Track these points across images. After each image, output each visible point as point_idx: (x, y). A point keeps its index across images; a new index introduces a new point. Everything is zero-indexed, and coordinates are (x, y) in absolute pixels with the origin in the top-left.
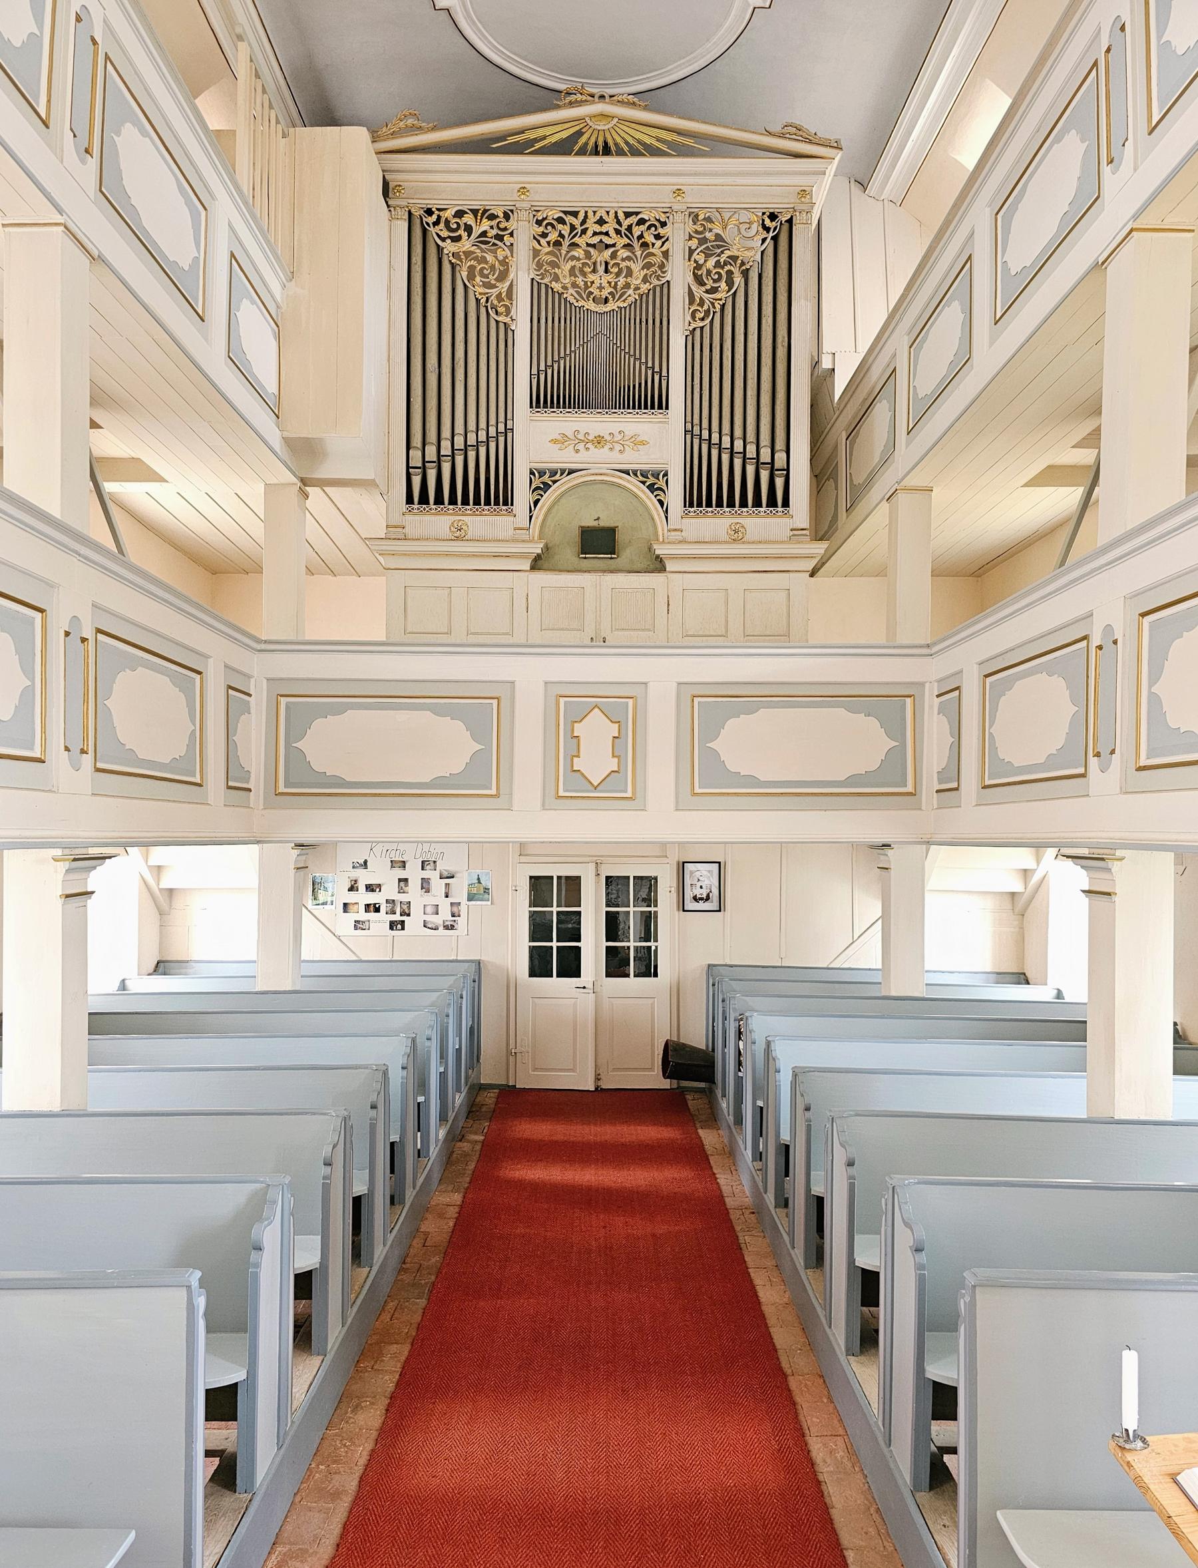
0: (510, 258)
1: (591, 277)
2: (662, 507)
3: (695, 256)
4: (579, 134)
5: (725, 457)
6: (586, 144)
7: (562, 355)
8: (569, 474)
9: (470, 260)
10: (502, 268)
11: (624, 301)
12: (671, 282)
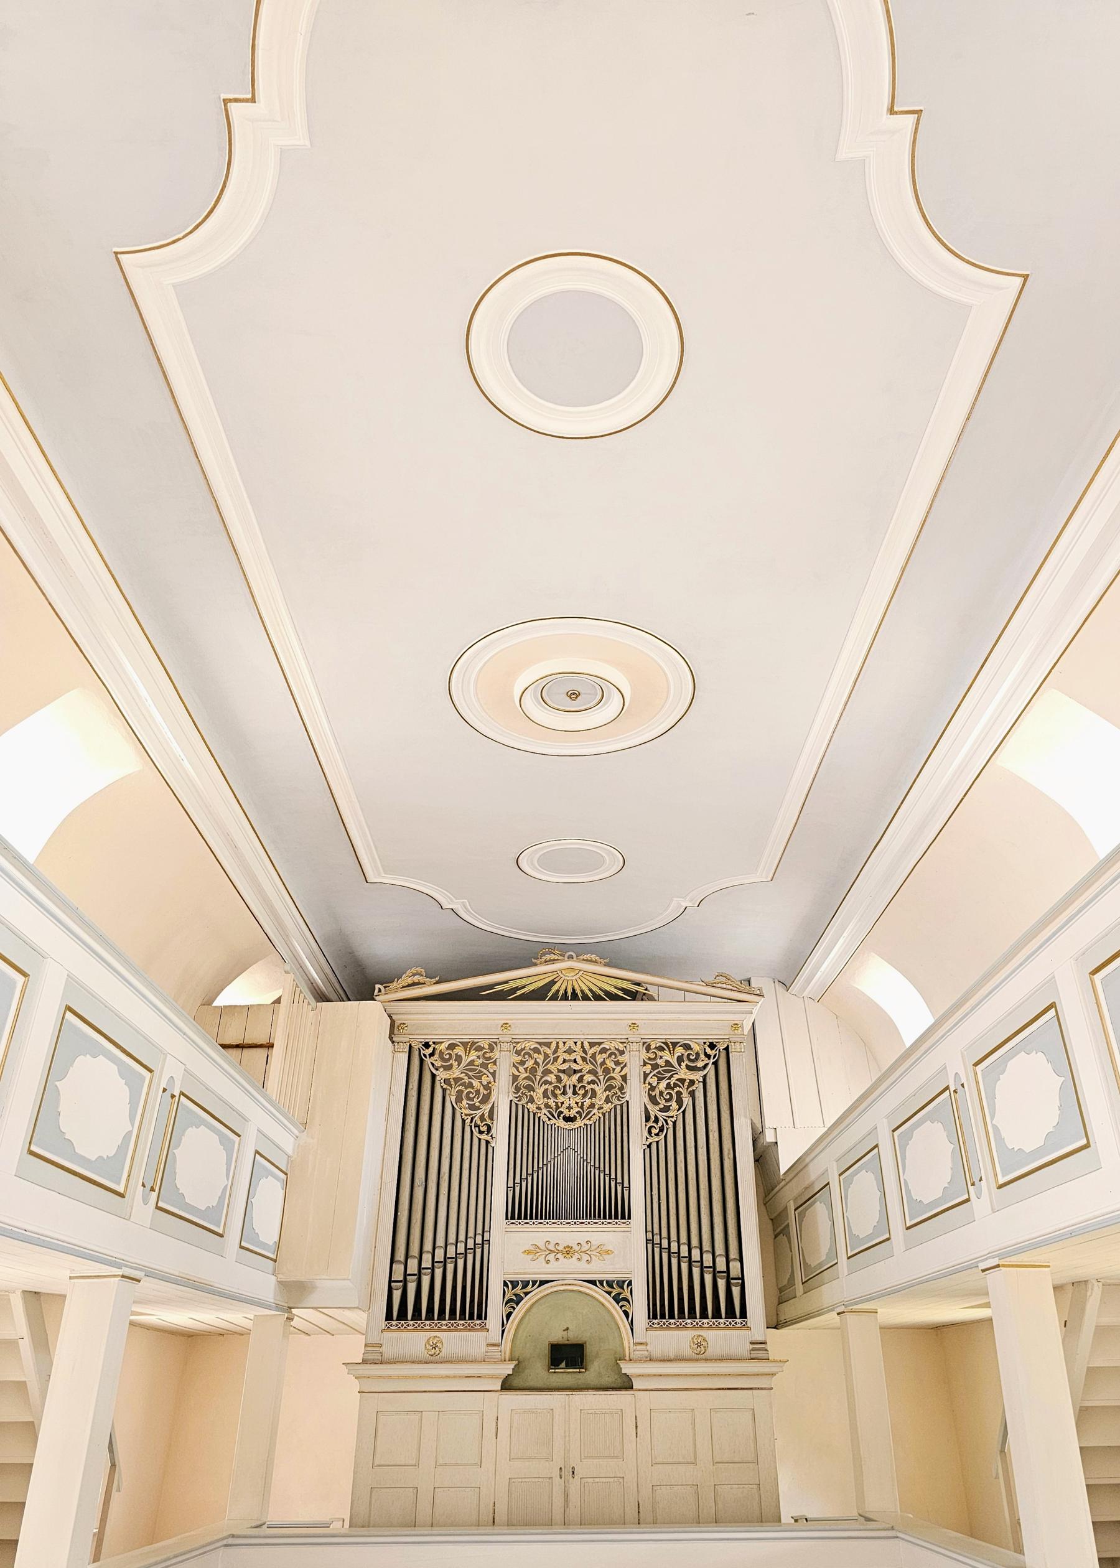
0: (493, 1083)
1: (561, 1099)
2: (627, 1318)
3: (649, 1079)
4: (553, 982)
5: (684, 1266)
6: (558, 991)
7: (536, 1168)
8: (538, 1287)
9: (459, 1086)
10: (485, 1092)
11: (589, 1119)
12: (630, 1102)
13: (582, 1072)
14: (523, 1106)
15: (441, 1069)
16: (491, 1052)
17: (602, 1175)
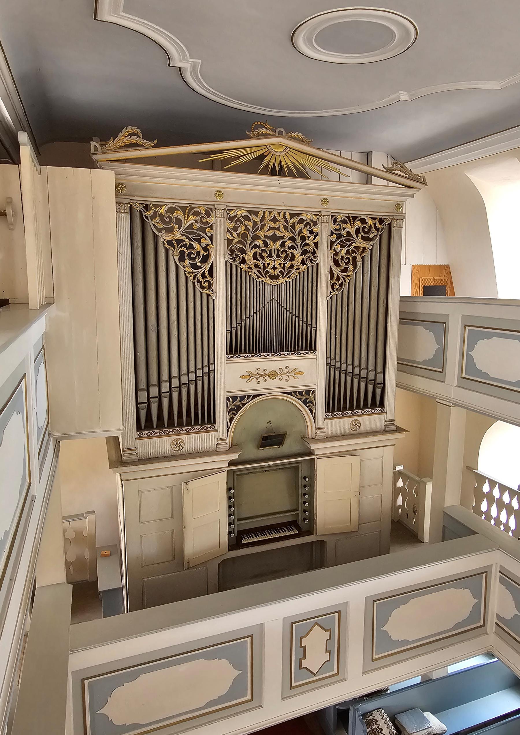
0: (211, 246)
1: (268, 261)
3: (334, 246)
7: (248, 315)
9: (181, 247)
13: (283, 238)
14: (236, 266)
15: (164, 232)
16: (208, 217)
17: (297, 319)
